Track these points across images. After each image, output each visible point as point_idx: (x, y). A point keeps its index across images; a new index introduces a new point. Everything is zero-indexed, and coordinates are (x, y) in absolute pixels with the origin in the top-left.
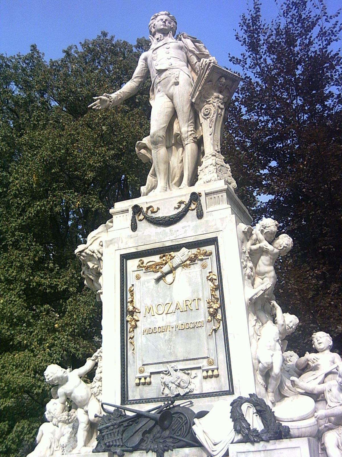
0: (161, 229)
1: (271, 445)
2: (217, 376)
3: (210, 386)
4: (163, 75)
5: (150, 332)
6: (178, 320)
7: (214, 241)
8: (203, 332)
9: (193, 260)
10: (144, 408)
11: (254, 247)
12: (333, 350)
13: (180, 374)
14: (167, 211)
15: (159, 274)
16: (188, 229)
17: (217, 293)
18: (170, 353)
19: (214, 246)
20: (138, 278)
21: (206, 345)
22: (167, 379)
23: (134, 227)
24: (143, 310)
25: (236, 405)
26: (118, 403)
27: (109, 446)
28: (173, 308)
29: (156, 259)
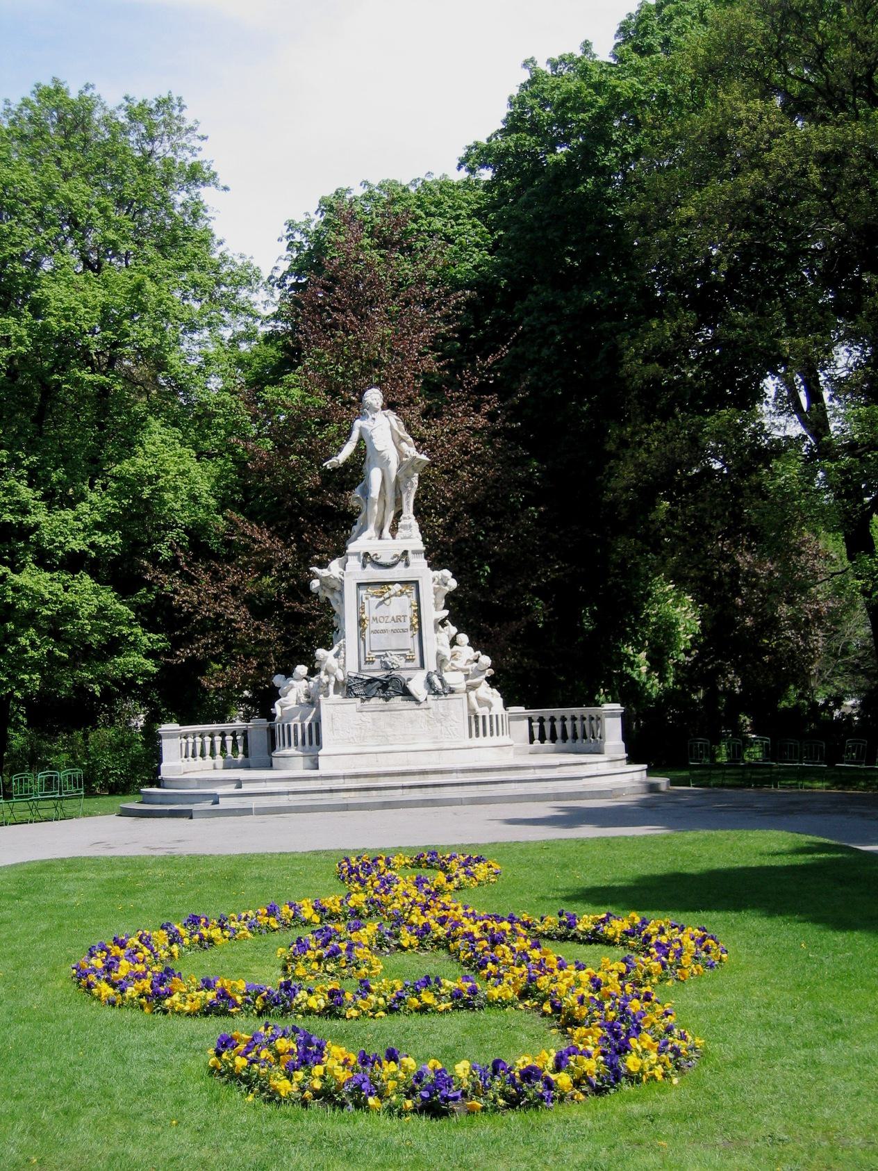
1: (449, 696)
5: (376, 632)
7: (417, 582)
9: (402, 593)
10: (375, 675)
16: (399, 573)
21: (411, 642)
23: (364, 566)
29: (378, 590)
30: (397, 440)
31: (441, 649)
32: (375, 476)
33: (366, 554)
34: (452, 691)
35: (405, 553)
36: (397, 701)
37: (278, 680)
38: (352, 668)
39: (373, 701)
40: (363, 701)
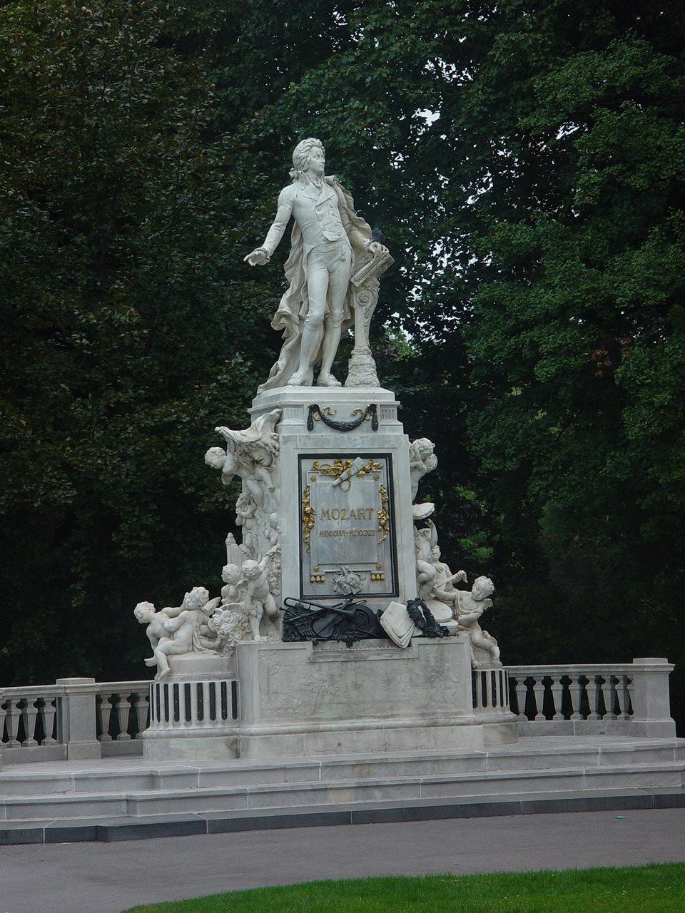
0: (338, 435)
2: (382, 580)
3: (376, 588)
4: (331, 247)
5: (326, 534)
6: (352, 526)
7: (388, 457)
8: (374, 540)
9: (367, 472)
10: (328, 603)
11: (415, 463)
12: (441, 560)
13: (352, 575)
14: (343, 417)
15: (337, 481)
17: (386, 506)
18: (345, 557)
19: (385, 460)
20: (313, 480)
22: (339, 579)
24: (319, 512)
25: (410, 605)
26: (298, 598)
27: (305, 636)
28: (347, 515)
29: (331, 462)
30: (347, 221)
31: (424, 564)
32: (317, 278)
33: (314, 408)
34: (446, 632)
35: (372, 408)
36: (367, 647)
37: (144, 609)
38: (290, 590)
39: (329, 646)
40: (315, 644)
